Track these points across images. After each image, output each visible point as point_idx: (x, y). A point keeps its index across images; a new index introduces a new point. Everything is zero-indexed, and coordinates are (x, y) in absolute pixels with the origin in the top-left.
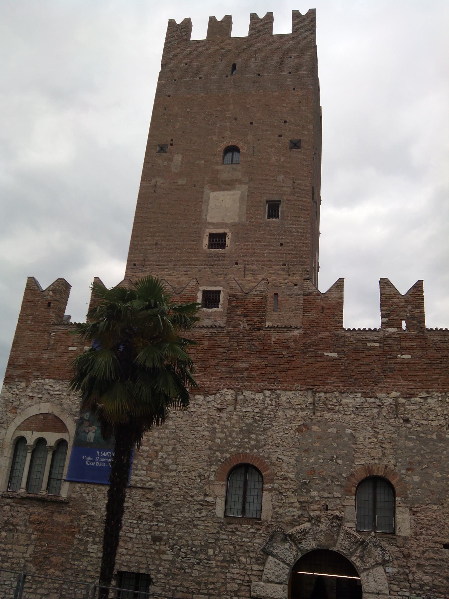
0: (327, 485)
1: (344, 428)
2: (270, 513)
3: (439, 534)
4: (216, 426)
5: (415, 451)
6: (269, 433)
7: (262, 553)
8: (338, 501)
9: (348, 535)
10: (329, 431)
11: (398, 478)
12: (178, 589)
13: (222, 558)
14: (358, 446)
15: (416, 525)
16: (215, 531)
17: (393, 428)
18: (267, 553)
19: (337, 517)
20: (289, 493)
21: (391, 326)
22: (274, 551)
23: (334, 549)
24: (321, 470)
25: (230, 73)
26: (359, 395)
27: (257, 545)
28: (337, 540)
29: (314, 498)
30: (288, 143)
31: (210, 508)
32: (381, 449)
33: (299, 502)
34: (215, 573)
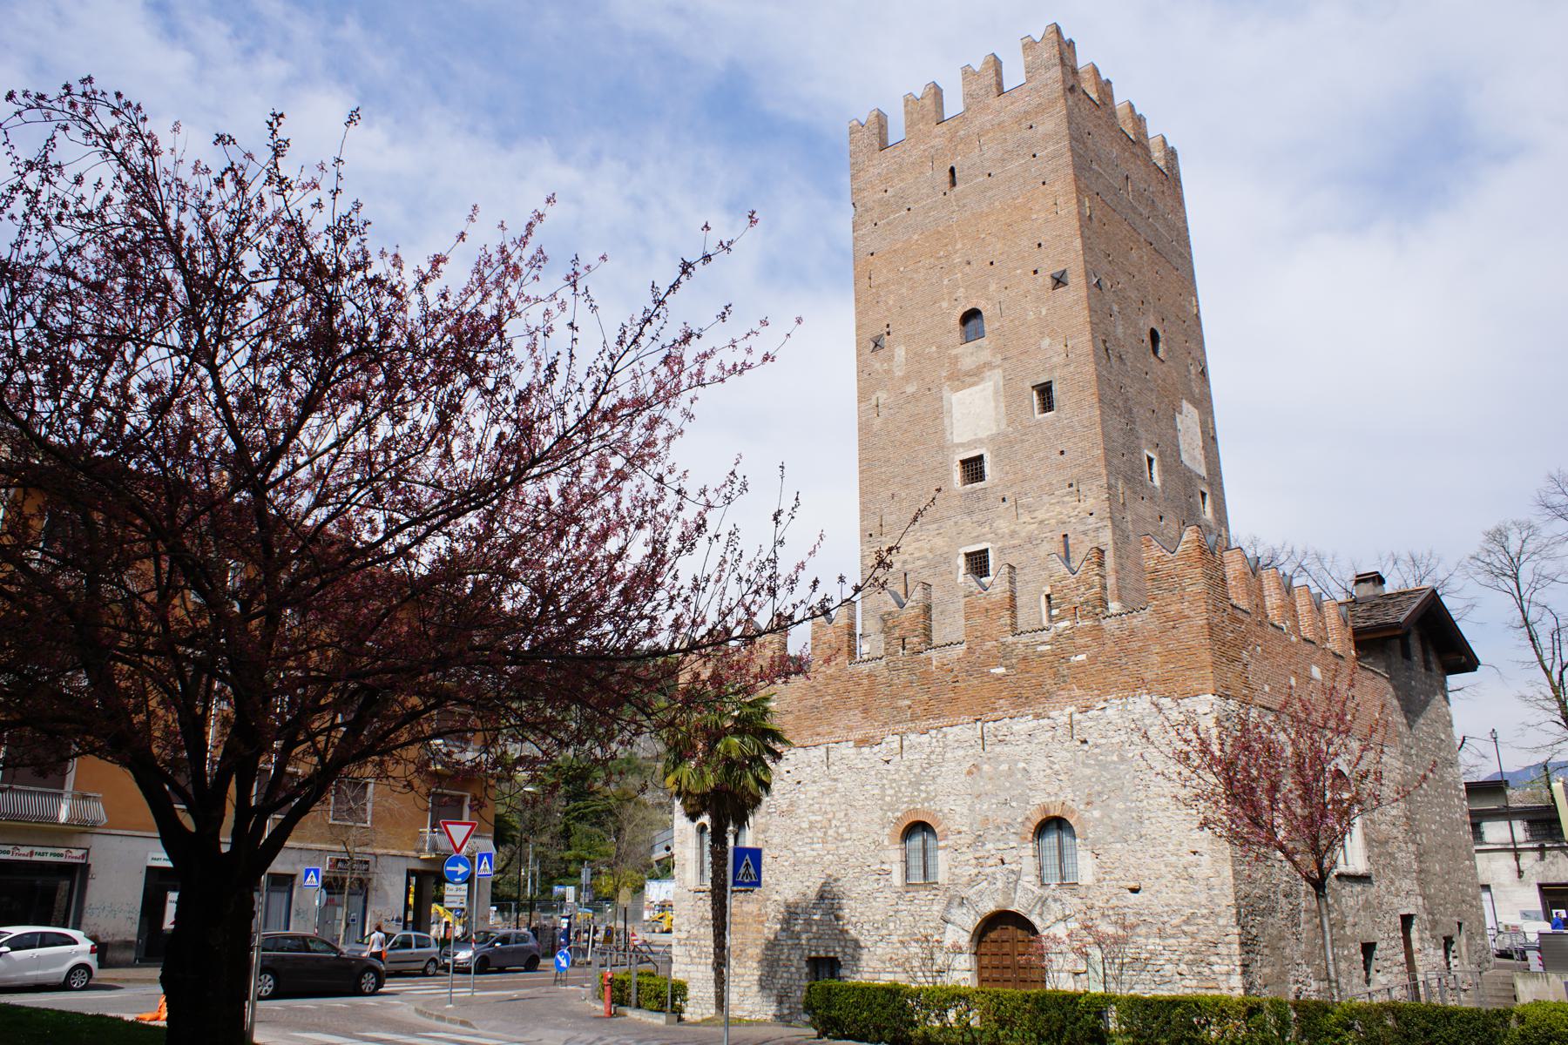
1: (1016, 762)
9: (1025, 890)
19: (1013, 872)
21: (1062, 619)
23: (1012, 909)
30: (1049, 282)
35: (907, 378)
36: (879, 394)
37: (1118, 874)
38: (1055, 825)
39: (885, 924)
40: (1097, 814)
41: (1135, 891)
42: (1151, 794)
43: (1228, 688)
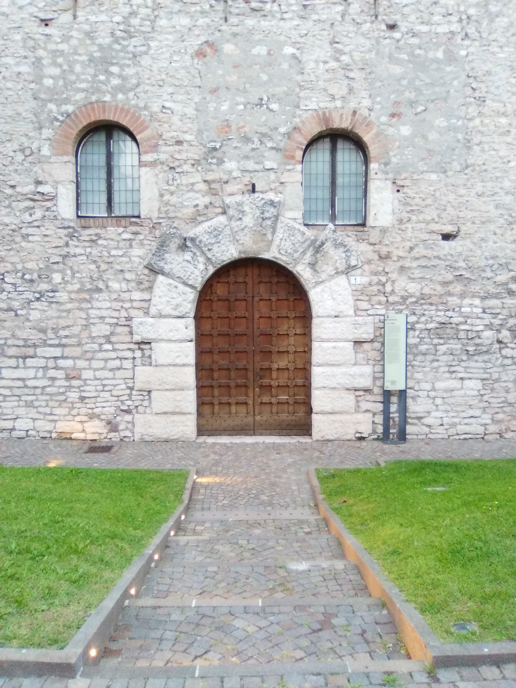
0: (253, 149)
1: (282, 45)
2: (156, 204)
3: (437, 220)
4: (41, 53)
5: (405, 82)
6: (143, 62)
7: (146, 271)
8: (272, 176)
10: (255, 51)
11: (374, 131)
12: (9, 342)
13: (77, 286)
14: (306, 77)
15: (402, 208)
16: (62, 243)
17: (368, 42)
18: (154, 271)
19: (272, 203)
20: (186, 167)
22: (167, 268)
23: (266, 256)
24: (242, 124)
27: (137, 260)
28: (272, 241)
29: (230, 172)
31: (48, 204)
32: (346, 82)
33: (205, 181)
34: (69, 311)
39: (44, 275)
40: (405, 131)
41: (446, 237)
42: (485, 110)
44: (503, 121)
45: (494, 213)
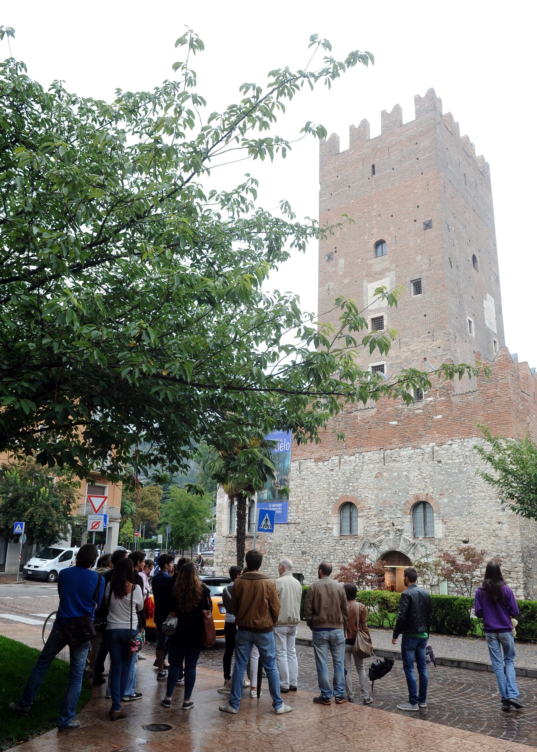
1: (402, 472)
2: (363, 531)
4: (330, 480)
8: (400, 520)
9: (406, 540)
19: (399, 530)
20: (372, 517)
21: (429, 396)
23: (398, 550)
25: (371, 174)
26: (410, 448)
30: (422, 225)
35: (345, 276)
36: (329, 283)
37: (457, 533)
38: (422, 506)
40: (446, 500)
42: (476, 490)
43: (519, 435)
44: (483, 494)
45: (482, 531)
